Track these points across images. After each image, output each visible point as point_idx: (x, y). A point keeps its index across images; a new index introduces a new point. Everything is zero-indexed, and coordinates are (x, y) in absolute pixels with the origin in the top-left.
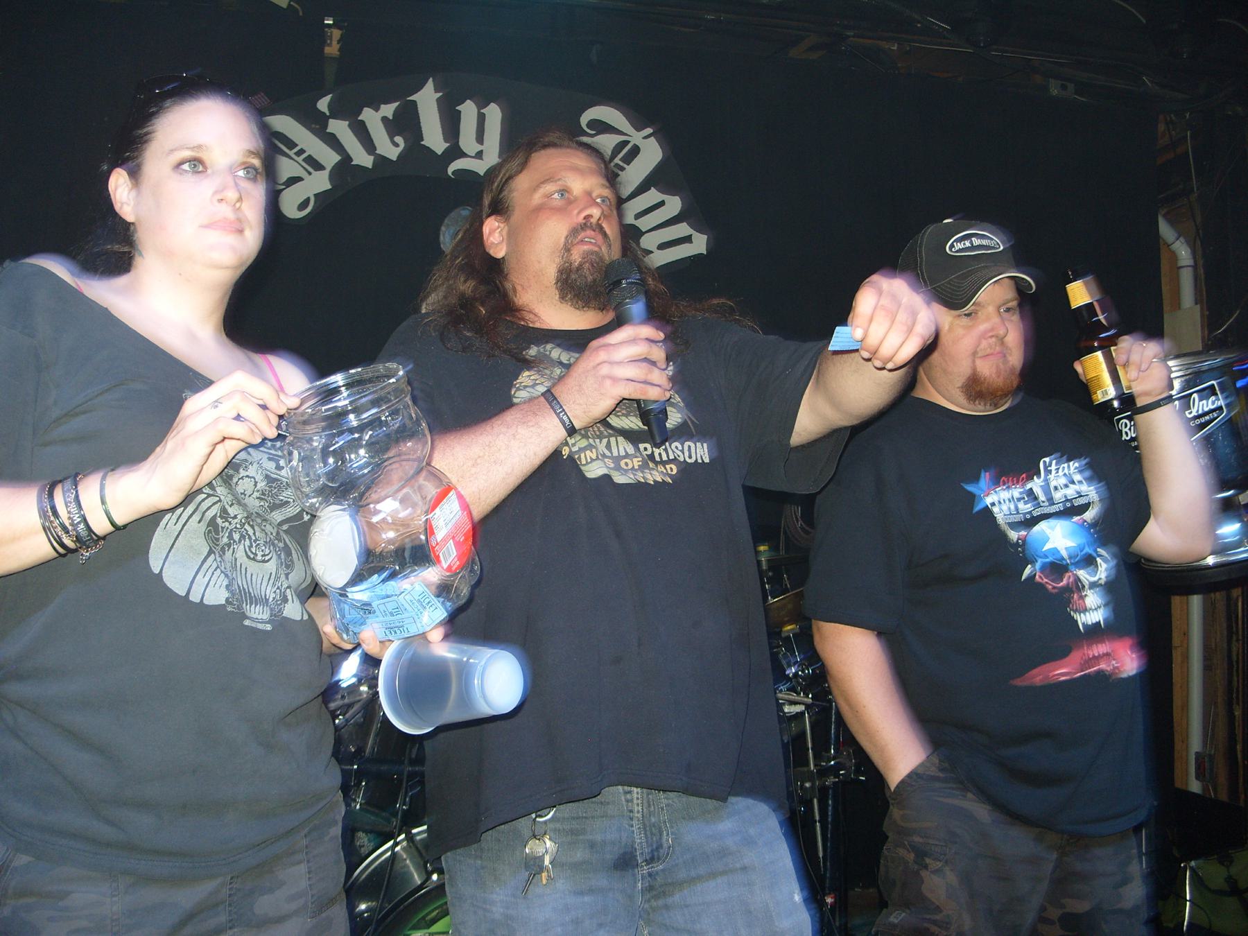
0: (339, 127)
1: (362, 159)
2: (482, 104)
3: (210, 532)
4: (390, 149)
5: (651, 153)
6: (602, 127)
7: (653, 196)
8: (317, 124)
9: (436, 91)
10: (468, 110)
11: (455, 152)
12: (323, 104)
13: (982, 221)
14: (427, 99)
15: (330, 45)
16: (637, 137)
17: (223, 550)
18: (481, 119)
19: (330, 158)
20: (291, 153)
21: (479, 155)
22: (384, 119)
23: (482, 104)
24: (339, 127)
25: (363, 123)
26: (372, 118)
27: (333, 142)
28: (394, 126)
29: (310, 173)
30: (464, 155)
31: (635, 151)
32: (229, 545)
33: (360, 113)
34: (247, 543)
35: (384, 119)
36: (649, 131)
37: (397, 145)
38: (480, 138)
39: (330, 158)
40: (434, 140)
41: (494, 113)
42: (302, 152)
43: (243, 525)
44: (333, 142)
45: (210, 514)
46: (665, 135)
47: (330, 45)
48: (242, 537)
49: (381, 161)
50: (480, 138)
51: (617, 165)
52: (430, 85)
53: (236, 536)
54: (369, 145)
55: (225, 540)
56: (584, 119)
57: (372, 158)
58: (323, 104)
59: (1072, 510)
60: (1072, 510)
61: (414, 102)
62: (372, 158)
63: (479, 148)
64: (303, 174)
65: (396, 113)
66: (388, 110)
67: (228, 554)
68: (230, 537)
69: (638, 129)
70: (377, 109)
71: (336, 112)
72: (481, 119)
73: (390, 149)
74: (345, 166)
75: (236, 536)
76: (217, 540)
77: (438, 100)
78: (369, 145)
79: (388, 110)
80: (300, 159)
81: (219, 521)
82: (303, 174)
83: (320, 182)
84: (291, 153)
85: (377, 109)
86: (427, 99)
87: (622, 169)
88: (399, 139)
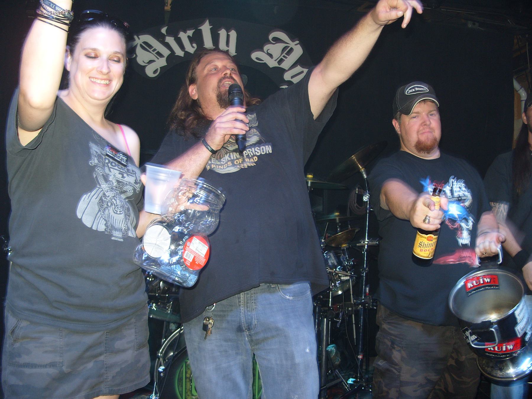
0: (170, 40)
1: (179, 53)
2: (228, 31)
3: (100, 202)
4: (191, 49)
5: (298, 51)
6: (277, 40)
7: (299, 69)
8: (161, 38)
10: (223, 33)
12: (164, 30)
13: (425, 83)
14: (206, 28)
15: (167, 6)
16: (292, 44)
17: (105, 210)
18: (228, 37)
19: (166, 52)
20: (151, 50)
22: (189, 37)
24: (170, 40)
25: (180, 38)
26: (183, 36)
27: (167, 46)
28: (191, 40)
29: (158, 59)
31: (291, 50)
32: (107, 208)
33: (178, 33)
34: (114, 207)
35: (189, 37)
36: (297, 42)
37: (193, 47)
39: (166, 52)
41: (233, 34)
42: (155, 50)
43: (111, 199)
44: (167, 46)
45: (100, 195)
46: (303, 44)
47: (167, 6)
48: (112, 204)
49: (187, 53)
51: (284, 56)
52: (207, 22)
53: (109, 204)
54: (182, 47)
55: (106, 206)
56: (271, 37)
57: (183, 53)
58: (164, 30)
59: (460, 200)
60: (460, 200)
61: (201, 30)
62: (183, 53)
64: (155, 59)
65: (194, 33)
66: (190, 33)
67: (107, 211)
68: (107, 205)
69: (293, 41)
70: (185, 32)
71: (169, 33)
72: (228, 37)
73: (191, 49)
74: (172, 57)
75: (109, 204)
76: (103, 206)
77: (211, 29)
78: (182, 47)
79: (190, 33)
80: (154, 53)
81: (103, 198)
82: (155, 59)
83: (162, 62)
84: (151, 50)
86: (206, 28)
87: (286, 58)
88: (195, 45)
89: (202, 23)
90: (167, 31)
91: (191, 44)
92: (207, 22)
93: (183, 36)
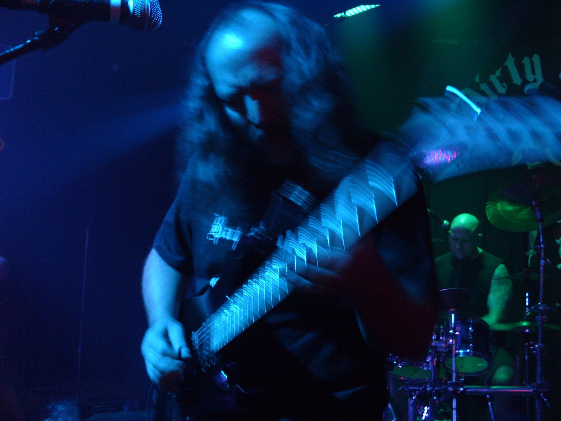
0: (484, 87)
2: (531, 57)
9: (513, 57)
10: (526, 61)
11: (526, 82)
12: (477, 80)
14: (510, 63)
18: (532, 63)
21: (535, 81)
22: (498, 78)
23: (531, 57)
24: (484, 87)
26: (493, 79)
30: (529, 82)
35: (498, 78)
37: (504, 87)
38: (534, 73)
40: (517, 81)
41: (536, 58)
50: (534, 73)
52: (510, 56)
63: (533, 77)
65: (502, 73)
66: (498, 73)
70: (494, 74)
72: (532, 63)
79: (498, 73)
85: (494, 74)
88: (504, 84)
89: (506, 59)
90: (480, 79)
91: (501, 83)
92: (510, 56)
93: (493, 79)
